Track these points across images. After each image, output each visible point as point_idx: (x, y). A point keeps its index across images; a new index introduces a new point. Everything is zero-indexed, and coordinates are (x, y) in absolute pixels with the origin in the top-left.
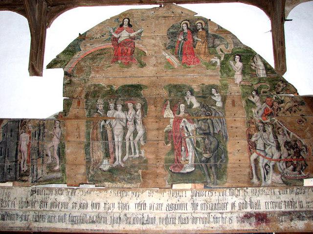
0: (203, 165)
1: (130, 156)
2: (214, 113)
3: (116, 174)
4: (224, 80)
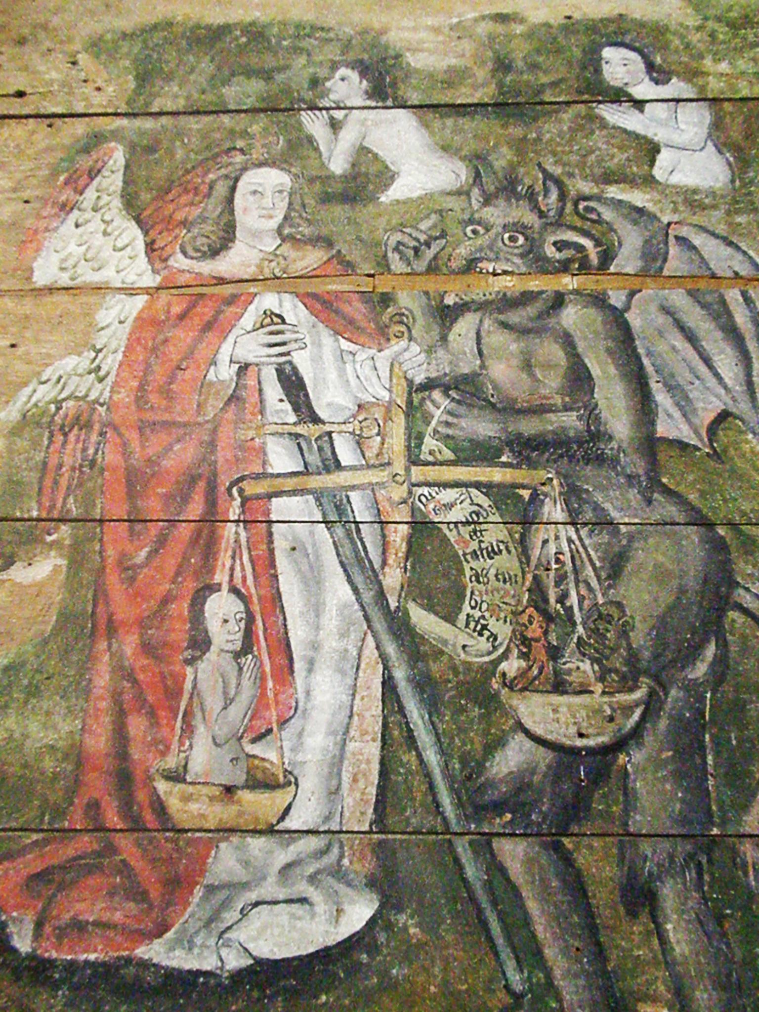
0: (514, 853)
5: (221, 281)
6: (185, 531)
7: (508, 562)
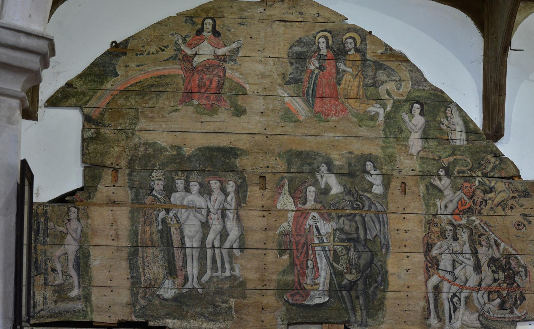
0: (344, 293)
1: (214, 275)
2: (367, 204)
3: (187, 305)
4: (387, 147)
5: (306, 210)
6: (304, 251)
7: (346, 257)
